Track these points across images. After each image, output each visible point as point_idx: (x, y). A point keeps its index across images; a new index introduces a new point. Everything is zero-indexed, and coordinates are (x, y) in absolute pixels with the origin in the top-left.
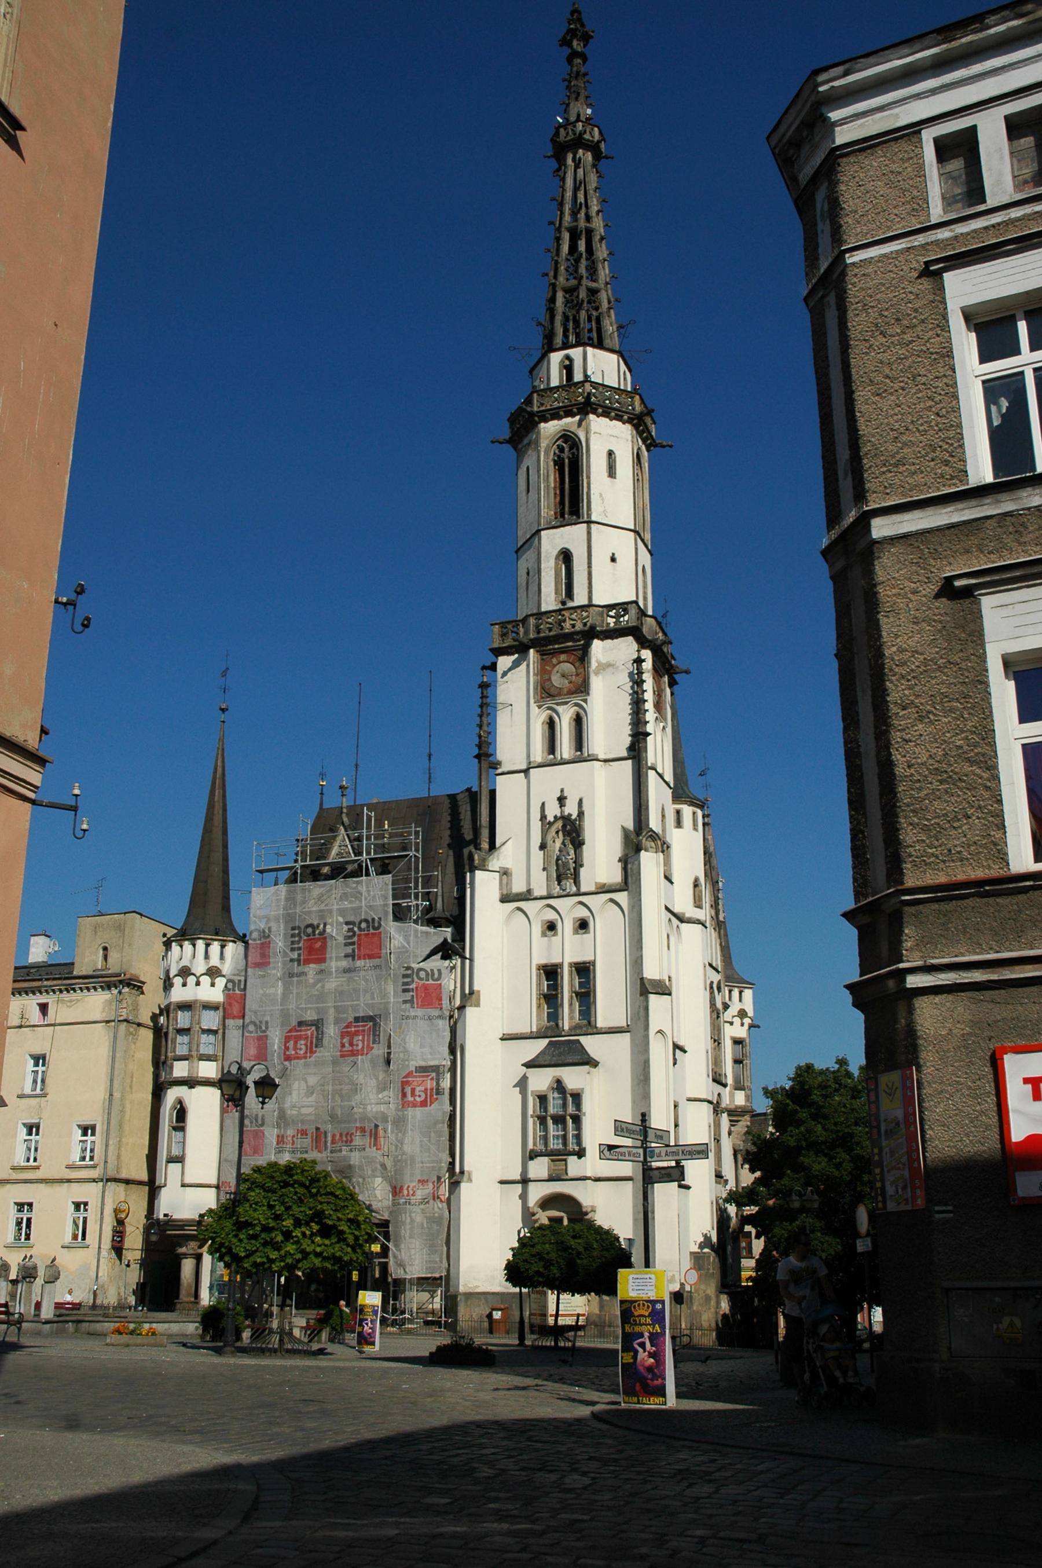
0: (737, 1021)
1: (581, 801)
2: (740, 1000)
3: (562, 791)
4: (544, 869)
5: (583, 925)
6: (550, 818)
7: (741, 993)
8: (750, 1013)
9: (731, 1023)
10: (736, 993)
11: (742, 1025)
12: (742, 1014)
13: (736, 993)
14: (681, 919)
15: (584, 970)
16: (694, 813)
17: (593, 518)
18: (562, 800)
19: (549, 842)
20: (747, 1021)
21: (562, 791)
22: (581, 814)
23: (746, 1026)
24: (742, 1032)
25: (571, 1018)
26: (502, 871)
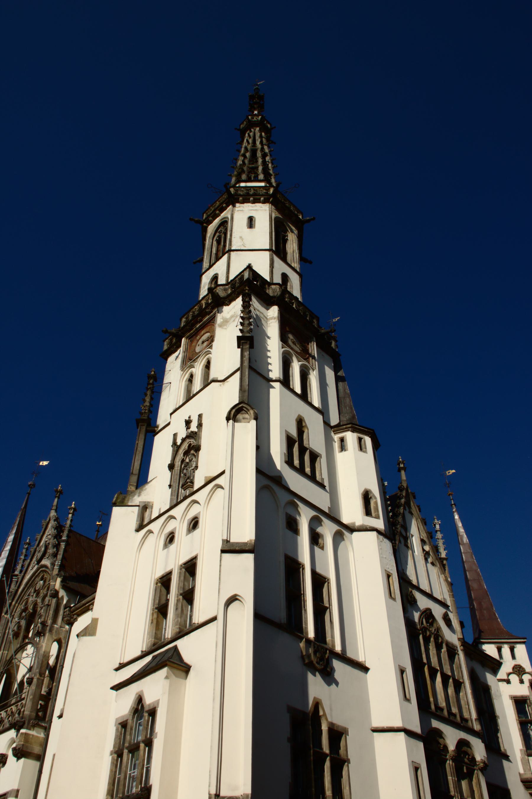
0: (514, 678)
1: (200, 416)
2: (514, 657)
3: (189, 417)
4: (170, 486)
5: (194, 524)
6: (179, 442)
7: (512, 650)
8: (528, 668)
9: (508, 682)
10: (506, 650)
11: (522, 682)
12: (519, 670)
13: (506, 650)
14: (351, 529)
15: (190, 568)
16: (360, 439)
17: (233, 248)
18: (188, 423)
19: (178, 463)
20: (526, 678)
21: (189, 417)
22: (200, 425)
23: (527, 684)
24: (523, 690)
25: (175, 624)
26: (142, 505)
